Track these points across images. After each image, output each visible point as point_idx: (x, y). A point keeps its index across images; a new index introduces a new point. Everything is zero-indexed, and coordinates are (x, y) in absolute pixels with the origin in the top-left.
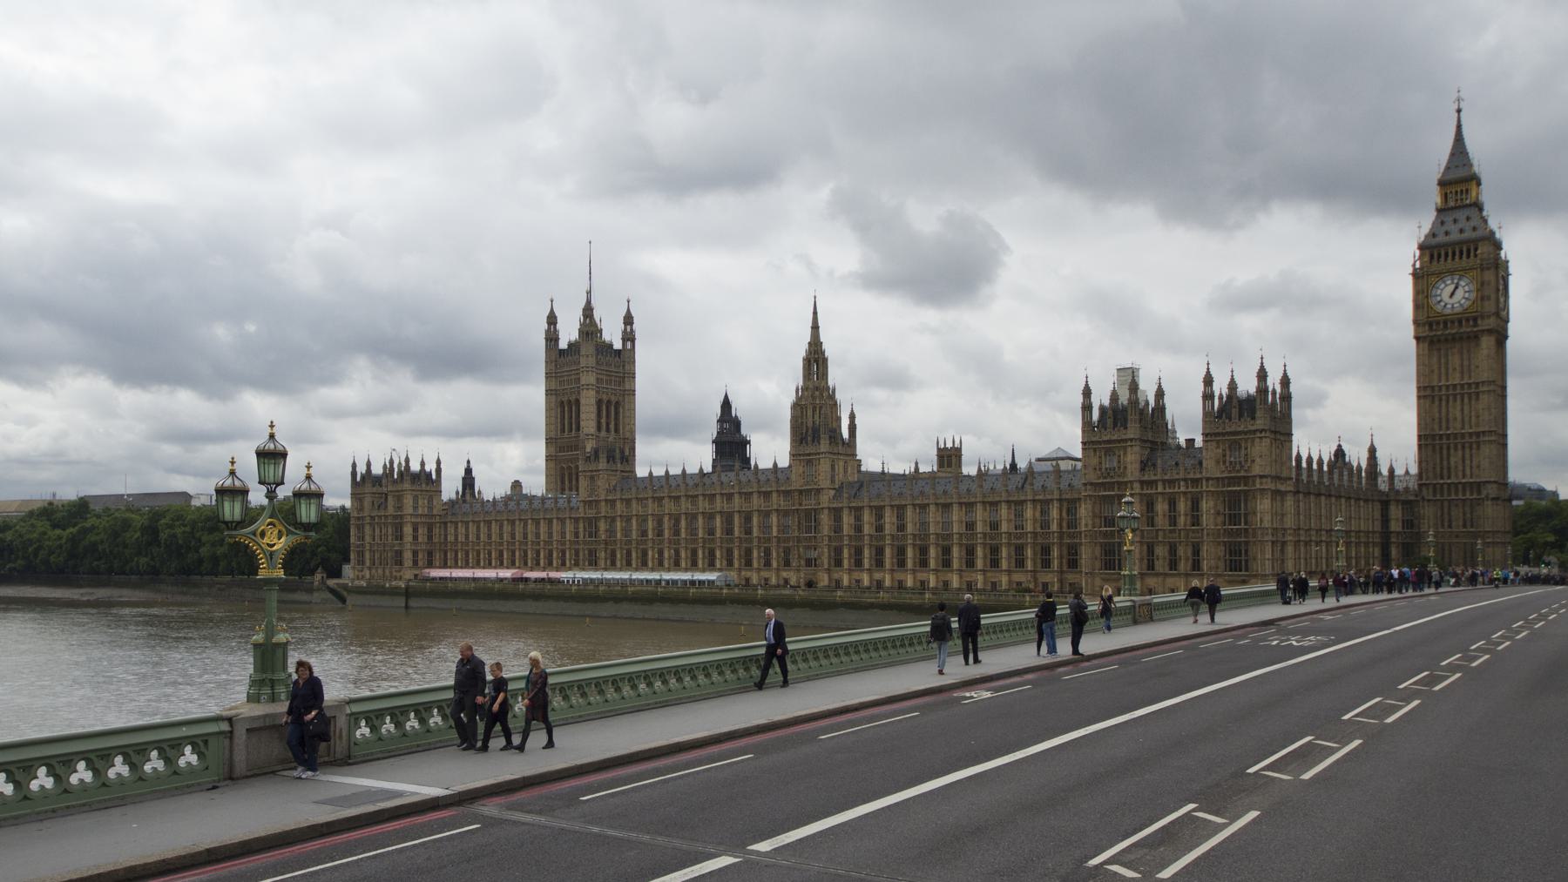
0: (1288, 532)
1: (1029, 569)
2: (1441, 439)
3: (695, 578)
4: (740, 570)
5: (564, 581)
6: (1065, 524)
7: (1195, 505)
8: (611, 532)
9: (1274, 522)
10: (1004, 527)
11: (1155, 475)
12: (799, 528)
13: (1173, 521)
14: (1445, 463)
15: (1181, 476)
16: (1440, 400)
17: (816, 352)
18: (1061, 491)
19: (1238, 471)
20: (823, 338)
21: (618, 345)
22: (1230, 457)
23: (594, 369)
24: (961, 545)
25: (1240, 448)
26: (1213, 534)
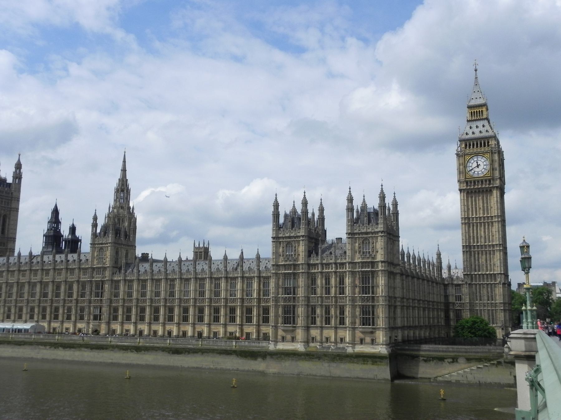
0: (398, 299)
1: (238, 323)
2: (474, 248)
3: (15, 327)
4: (50, 322)
6: (262, 294)
7: (342, 282)
10: (223, 295)
13: (328, 291)
14: (477, 262)
15: (333, 261)
16: (473, 226)
17: (123, 185)
20: (128, 177)
21: (10, 180)
25: (369, 243)
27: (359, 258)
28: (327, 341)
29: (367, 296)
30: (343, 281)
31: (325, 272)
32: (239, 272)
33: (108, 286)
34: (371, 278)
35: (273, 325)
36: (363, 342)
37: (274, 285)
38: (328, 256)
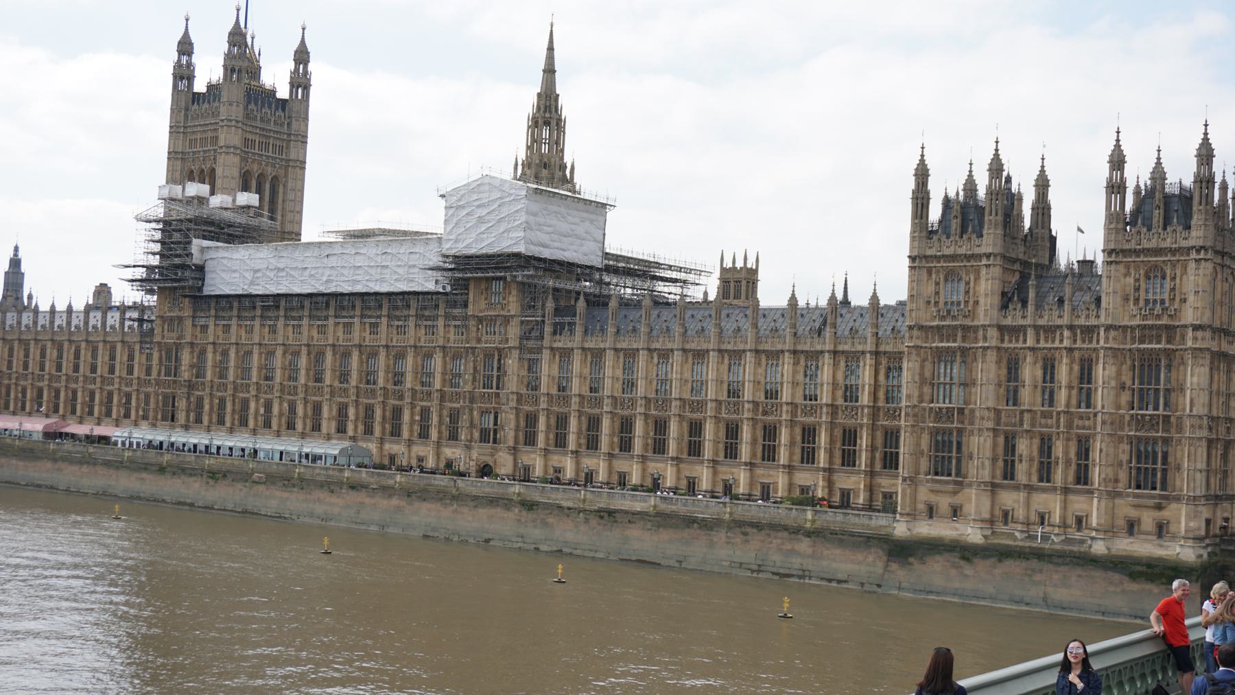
1: (822, 465)
3: (306, 450)
4: (382, 441)
5: (116, 443)
6: (881, 395)
7: (1086, 375)
8: (198, 368)
9: (1214, 406)
10: (786, 396)
11: (1024, 317)
12: (474, 380)
15: (1065, 321)
18: (878, 339)
19: (1158, 317)
21: (283, 92)
22: (1147, 291)
23: (240, 125)
24: (717, 419)
25: (1164, 278)
26: (1112, 423)
27: (1135, 316)
28: (1042, 523)
29: (1150, 415)
30: (1090, 374)
31: (1044, 348)
32: (827, 340)
33: (513, 362)
34: (1163, 369)
35: (906, 476)
36: (1136, 528)
37: (910, 377)
38: (1051, 309)
